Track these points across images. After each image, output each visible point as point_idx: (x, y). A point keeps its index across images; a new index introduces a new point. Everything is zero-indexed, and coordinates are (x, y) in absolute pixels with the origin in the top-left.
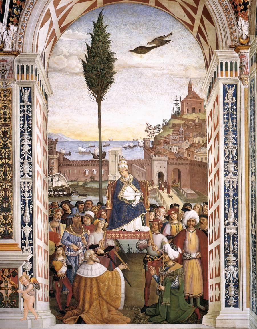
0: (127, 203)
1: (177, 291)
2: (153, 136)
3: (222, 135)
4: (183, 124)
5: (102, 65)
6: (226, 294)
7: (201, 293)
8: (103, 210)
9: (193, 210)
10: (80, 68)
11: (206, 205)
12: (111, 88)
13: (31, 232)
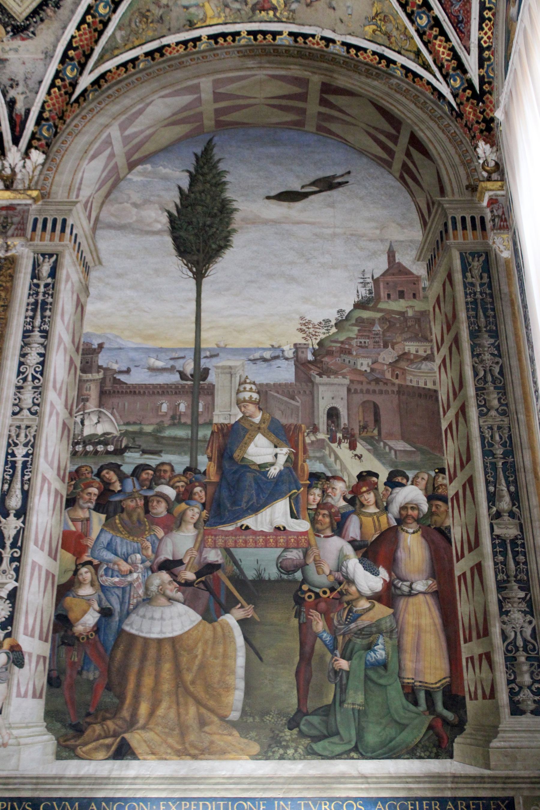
0: (255, 470)
1: (382, 672)
2: (314, 341)
3: (466, 340)
4: (379, 319)
5: (209, 219)
6: (509, 682)
7: (444, 678)
8: (197, 484)
9: (412, 484)
11: (441, 475)
12: (223, 256)
13: (20, 534)
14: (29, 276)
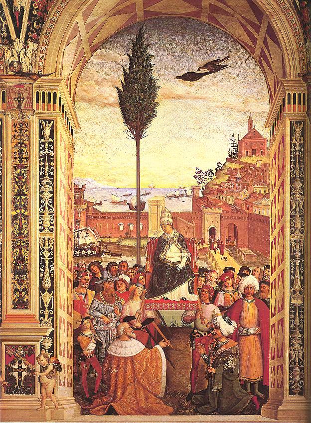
1: (231, 374)
4: (240, 169)
6: (290, 379)
10: (114, 97)
13: (52, 301)
14: (38, 136)
